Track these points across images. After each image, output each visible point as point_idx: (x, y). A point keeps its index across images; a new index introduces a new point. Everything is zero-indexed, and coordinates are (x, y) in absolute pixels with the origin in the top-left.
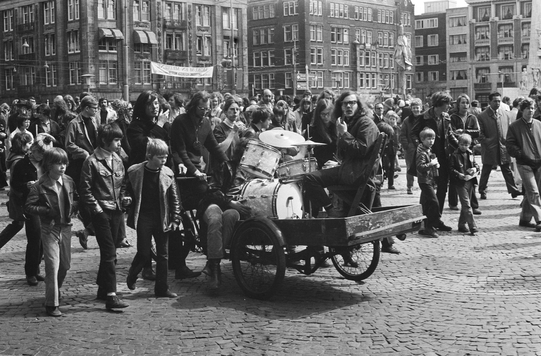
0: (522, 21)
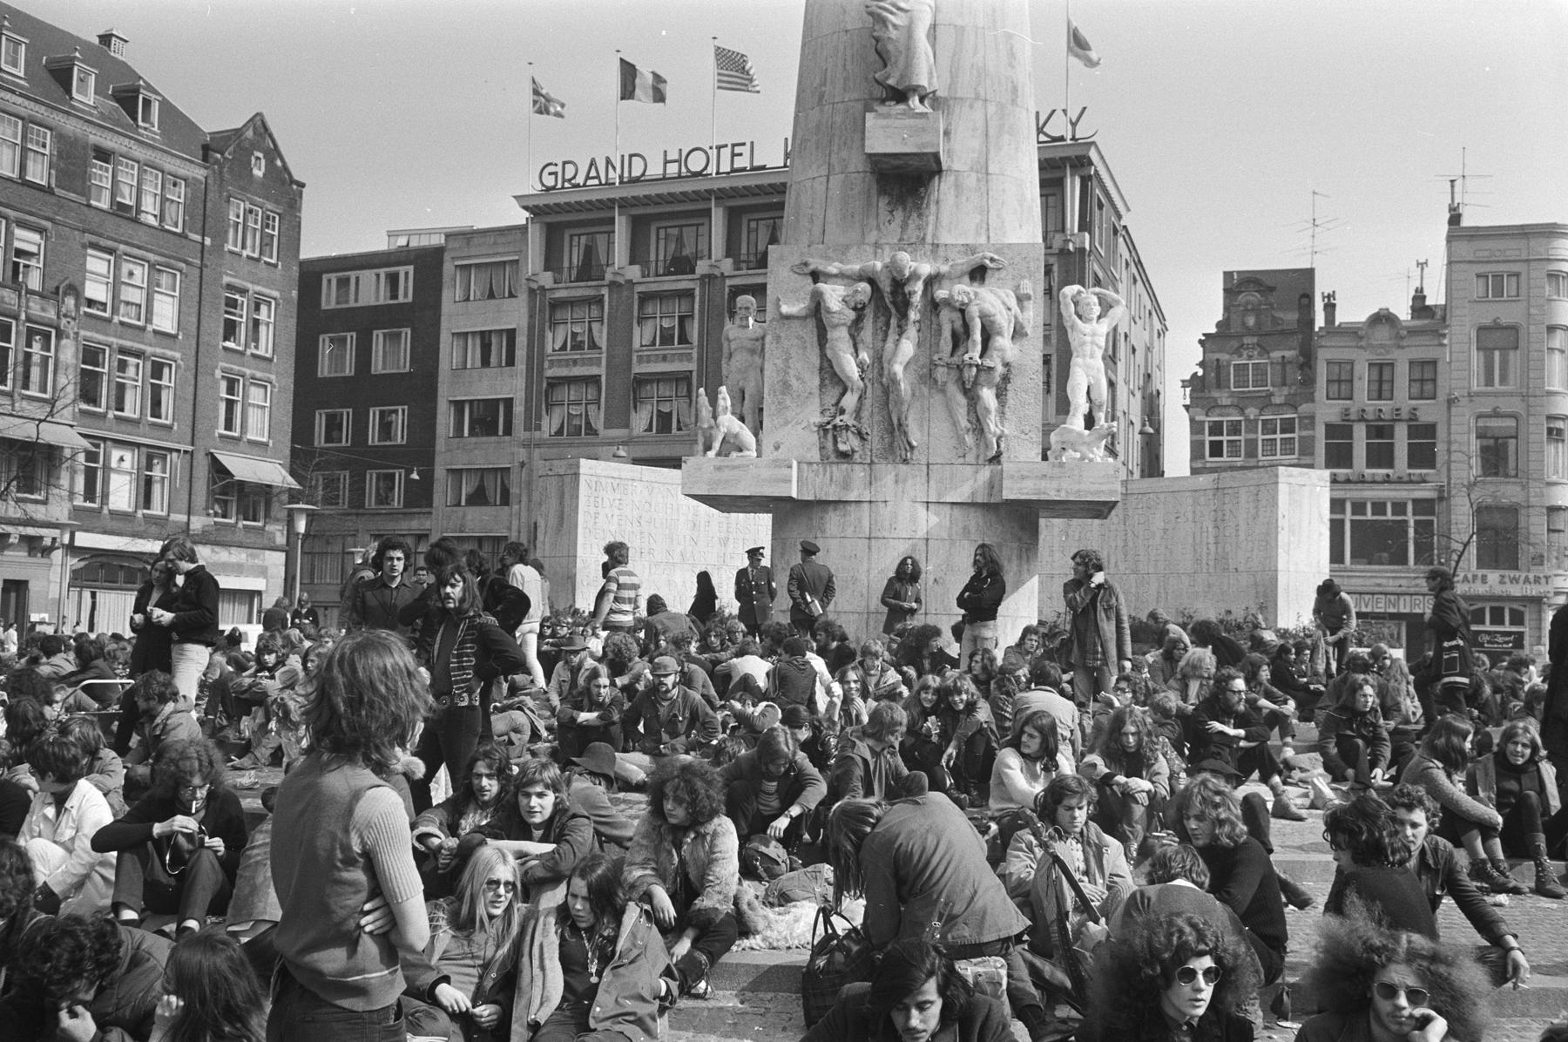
0: (728, 282)
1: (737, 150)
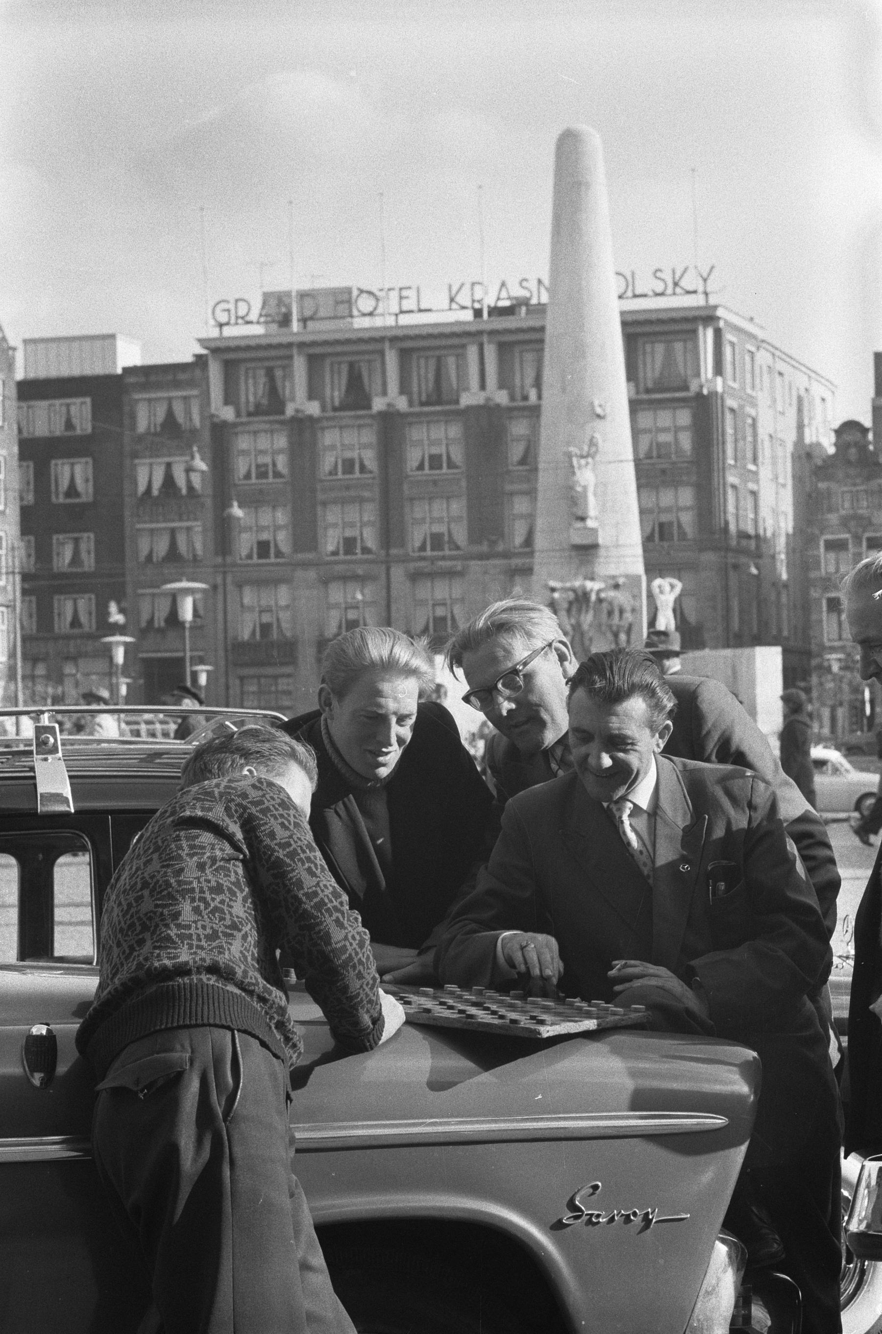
1: (405, 293)
